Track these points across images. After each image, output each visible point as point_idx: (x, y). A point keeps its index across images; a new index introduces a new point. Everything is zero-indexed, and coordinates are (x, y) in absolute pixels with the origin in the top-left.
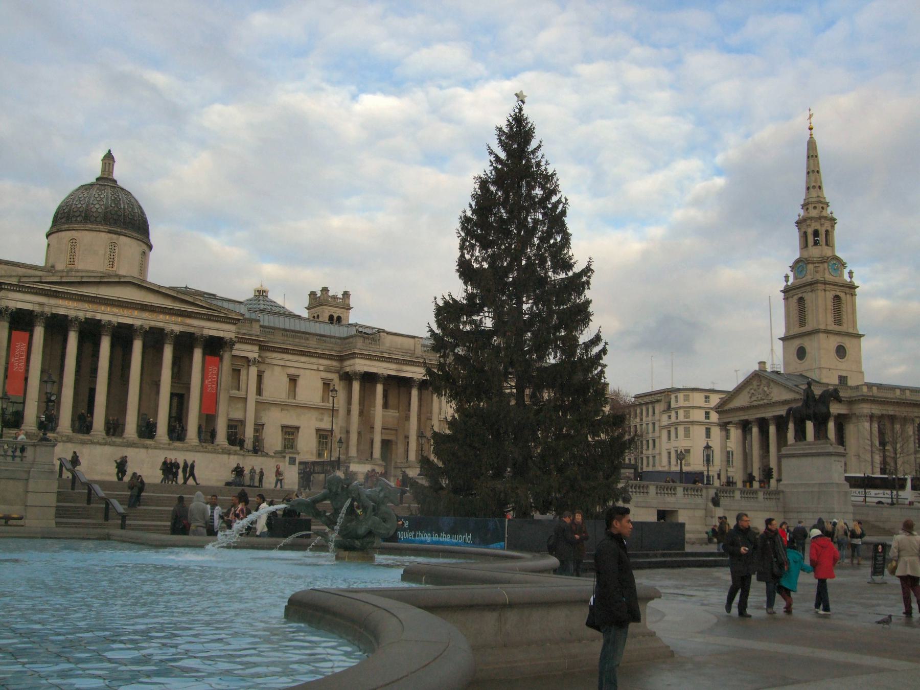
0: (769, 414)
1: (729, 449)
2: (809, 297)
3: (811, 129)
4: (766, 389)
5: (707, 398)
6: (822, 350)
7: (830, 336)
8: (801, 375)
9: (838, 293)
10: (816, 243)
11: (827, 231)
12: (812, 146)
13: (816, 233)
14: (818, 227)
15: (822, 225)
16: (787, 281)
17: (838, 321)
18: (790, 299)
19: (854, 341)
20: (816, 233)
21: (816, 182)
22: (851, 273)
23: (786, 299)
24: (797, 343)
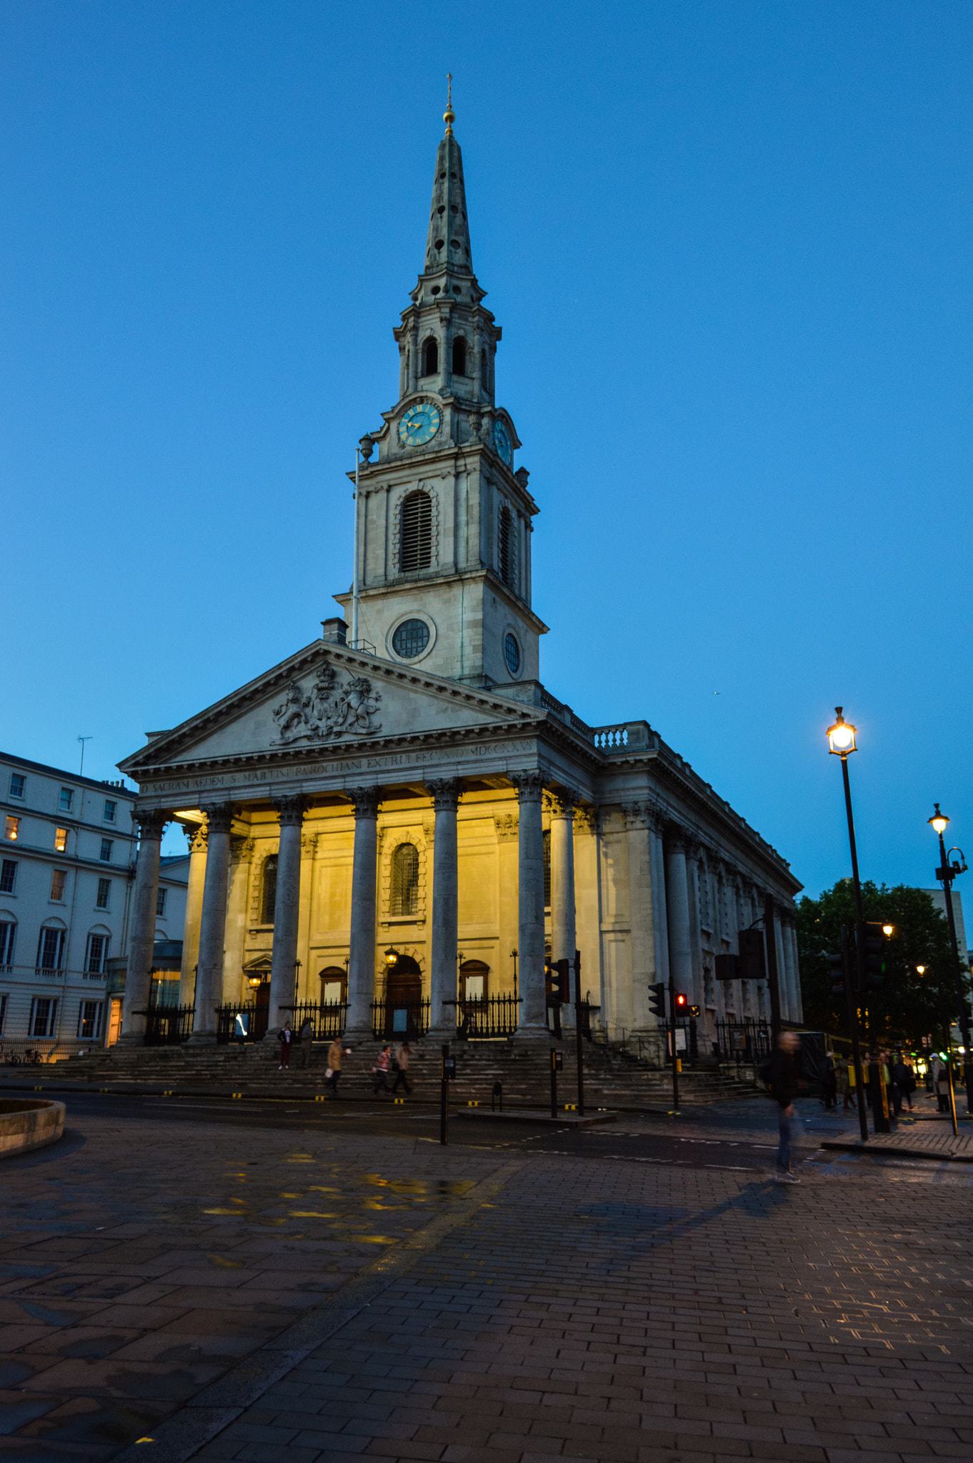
7: (498, 599)
9: (510, 507)
10: (458, 368)
11: (483, 351)
12: (452, 150)
19: (530, 635)
20: (459, 348)
22: (523, 472)
24: (399, 608)
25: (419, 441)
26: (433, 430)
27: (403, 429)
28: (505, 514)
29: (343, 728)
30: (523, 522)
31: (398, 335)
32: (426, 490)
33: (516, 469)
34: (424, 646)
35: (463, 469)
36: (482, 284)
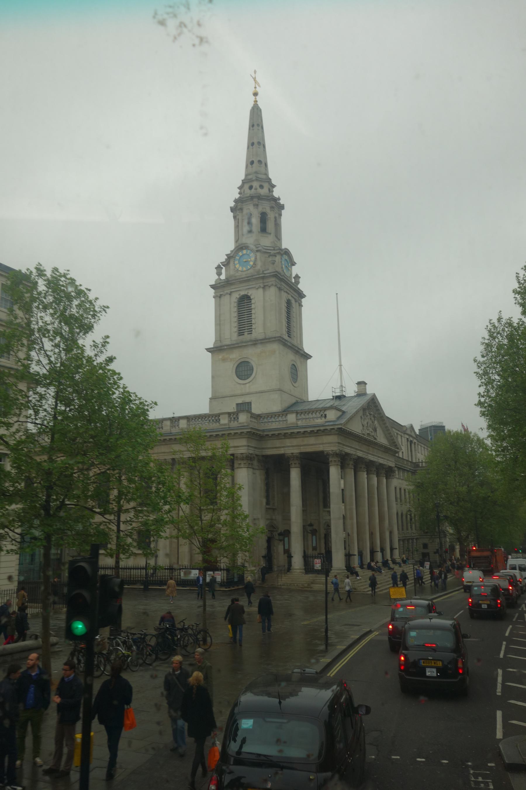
2: (257, 296)
3: (255, 94)
6: (268, 368)
9: (291, 298)
11: (275, 218)
12: (256, 113)
14: (268, 210)
15: (272, 208)
16: (219, 274)
18: (226, 299)
22: (297, 277)
23: (218, 297)
25: (244, 269)
26: (252, 263)
27: (237, 262)
28: (289, 302)
30: (297, 304)
31: (232, 210)
32: (249, 295)
33: (294, 275)
34: (251, 375)
35: (266, 284)
36: (274, 182)
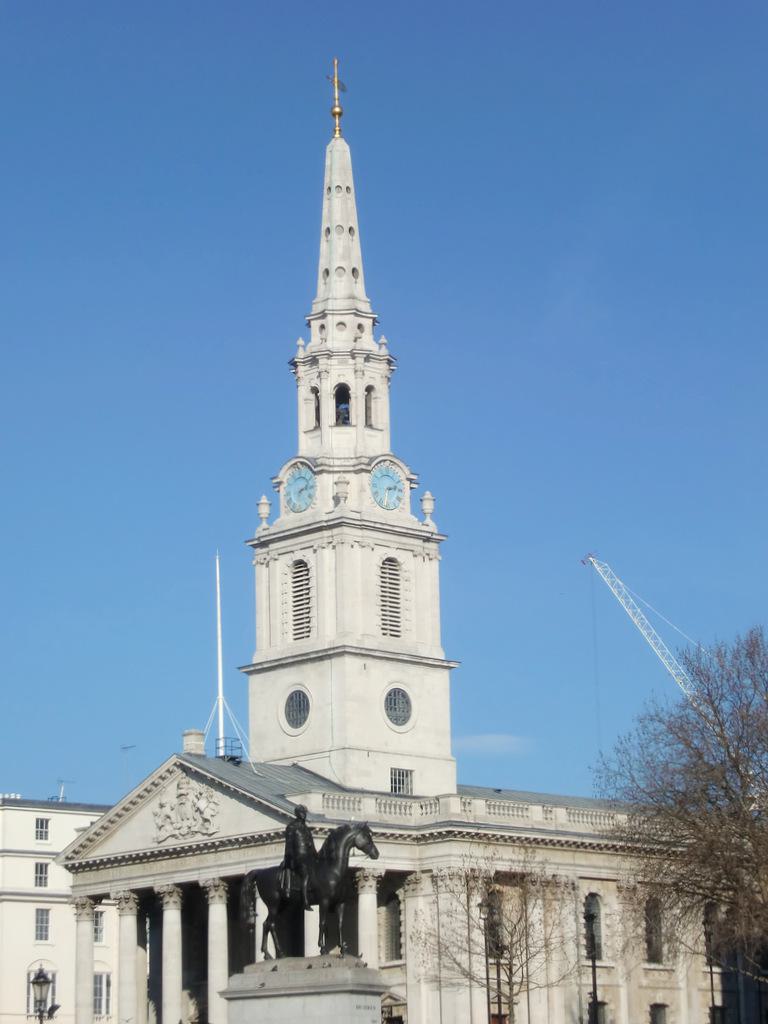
0: (208, 871)
1: (99, 969)
4: (202, 804)
5: (42, 824)
7: (369, 662)
8: (294, 765)
10: (343, 419)
13: (342, 394)
17: (391, 625)
20: (342, 394)
21: (347, 256)
29: (196, 829)
